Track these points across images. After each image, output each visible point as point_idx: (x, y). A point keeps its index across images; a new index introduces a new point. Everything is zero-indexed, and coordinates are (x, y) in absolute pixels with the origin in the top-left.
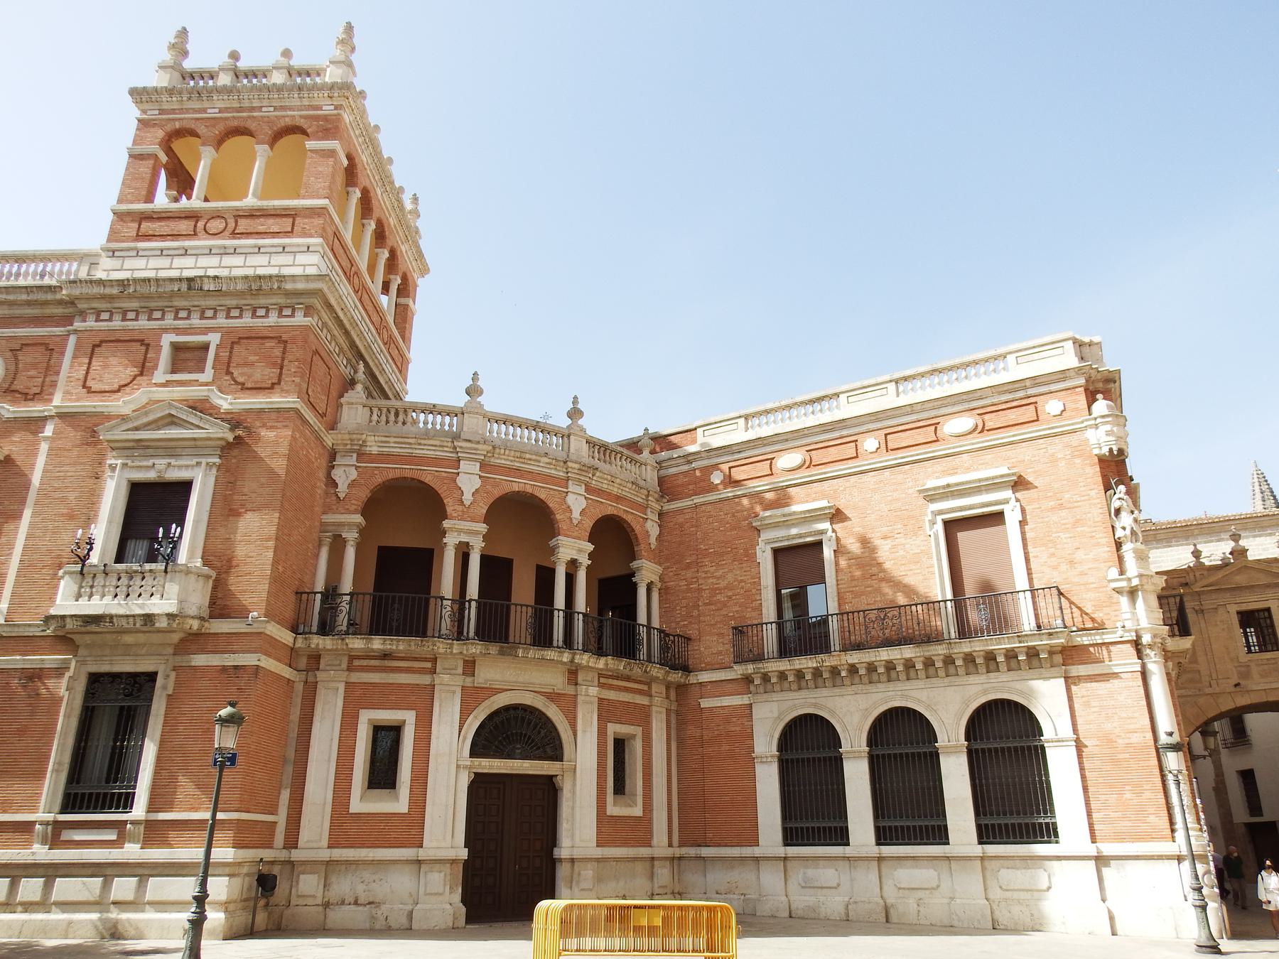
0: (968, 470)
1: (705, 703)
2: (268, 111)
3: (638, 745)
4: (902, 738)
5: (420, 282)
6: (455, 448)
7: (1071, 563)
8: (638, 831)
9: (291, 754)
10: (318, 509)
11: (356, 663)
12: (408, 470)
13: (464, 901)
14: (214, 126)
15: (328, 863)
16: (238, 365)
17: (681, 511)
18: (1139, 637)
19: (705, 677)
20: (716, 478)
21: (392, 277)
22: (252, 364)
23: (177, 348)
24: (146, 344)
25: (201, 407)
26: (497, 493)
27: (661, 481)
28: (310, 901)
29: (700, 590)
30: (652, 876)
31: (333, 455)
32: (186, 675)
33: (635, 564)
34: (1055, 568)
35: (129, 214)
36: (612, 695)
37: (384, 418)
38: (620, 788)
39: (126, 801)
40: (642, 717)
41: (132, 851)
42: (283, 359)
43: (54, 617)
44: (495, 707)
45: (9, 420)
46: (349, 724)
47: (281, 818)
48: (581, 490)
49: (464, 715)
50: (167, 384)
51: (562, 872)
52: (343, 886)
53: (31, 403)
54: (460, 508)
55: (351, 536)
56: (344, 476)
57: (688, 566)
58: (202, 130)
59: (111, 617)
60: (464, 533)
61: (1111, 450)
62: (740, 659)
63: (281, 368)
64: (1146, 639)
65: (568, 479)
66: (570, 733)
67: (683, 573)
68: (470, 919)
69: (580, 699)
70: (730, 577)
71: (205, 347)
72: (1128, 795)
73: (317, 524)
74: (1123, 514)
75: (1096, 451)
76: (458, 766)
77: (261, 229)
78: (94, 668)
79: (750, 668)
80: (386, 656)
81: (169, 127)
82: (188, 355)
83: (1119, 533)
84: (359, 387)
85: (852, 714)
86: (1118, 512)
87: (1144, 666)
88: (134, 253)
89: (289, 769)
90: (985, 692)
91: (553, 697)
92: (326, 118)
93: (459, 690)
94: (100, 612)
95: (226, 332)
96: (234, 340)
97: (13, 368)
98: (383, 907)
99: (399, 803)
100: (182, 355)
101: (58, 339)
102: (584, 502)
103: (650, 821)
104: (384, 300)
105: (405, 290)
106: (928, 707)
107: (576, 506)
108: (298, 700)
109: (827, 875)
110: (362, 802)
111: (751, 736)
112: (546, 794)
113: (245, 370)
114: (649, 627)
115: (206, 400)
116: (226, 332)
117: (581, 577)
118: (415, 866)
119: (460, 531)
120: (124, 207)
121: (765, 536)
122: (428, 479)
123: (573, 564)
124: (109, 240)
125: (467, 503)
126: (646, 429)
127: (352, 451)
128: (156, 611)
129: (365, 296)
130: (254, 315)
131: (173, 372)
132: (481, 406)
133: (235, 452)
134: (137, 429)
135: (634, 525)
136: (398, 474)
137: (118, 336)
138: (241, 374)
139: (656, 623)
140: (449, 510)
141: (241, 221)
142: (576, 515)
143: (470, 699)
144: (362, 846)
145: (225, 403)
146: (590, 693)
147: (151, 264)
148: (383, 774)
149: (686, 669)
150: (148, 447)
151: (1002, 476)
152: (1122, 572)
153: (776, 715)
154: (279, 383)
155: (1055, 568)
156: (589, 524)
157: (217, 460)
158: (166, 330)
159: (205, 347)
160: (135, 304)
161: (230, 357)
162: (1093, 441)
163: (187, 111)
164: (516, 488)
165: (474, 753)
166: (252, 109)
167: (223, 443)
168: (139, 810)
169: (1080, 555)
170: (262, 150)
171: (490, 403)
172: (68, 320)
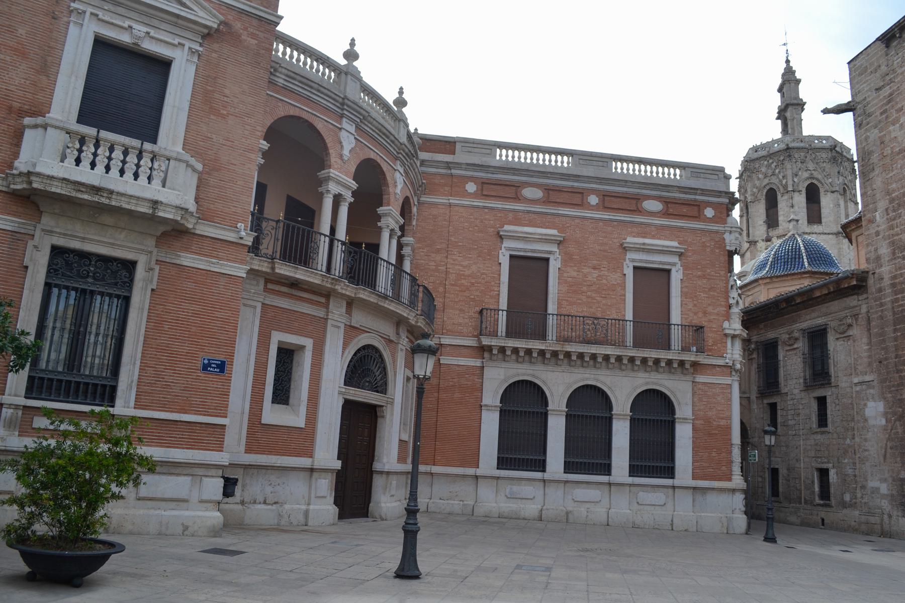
0: (653, 237)
4: (589, 407)
6: (343, 104)
7: (705, 313)
11: (270, 286)
13: (335, 503)
32: (172, 274)
34: (695, 314)
49: (345, 345)
54: (339, 161)
57: (438, 251)
59: (111, 192)
67: (433, 255)
68: (341, 516)
70: (474, 268)
72: (714, 454)
75: (728, 248)
78: (61, 242)
85: (559, 385)
90: (647, 383)
98: (287, 507)
106: (610, 388)
109: (527, 490)
110: (272, 415)
111: (481, 390)
118: (307, 474)
121: (507, 244)
122: (319, 126)
133: (216, 46)
144: (270, 452)
151: (673, 247)
153: (502, 377)
162: (727, 241)
165: (346, 383)
167: (206, 31)
169: (710, 309)
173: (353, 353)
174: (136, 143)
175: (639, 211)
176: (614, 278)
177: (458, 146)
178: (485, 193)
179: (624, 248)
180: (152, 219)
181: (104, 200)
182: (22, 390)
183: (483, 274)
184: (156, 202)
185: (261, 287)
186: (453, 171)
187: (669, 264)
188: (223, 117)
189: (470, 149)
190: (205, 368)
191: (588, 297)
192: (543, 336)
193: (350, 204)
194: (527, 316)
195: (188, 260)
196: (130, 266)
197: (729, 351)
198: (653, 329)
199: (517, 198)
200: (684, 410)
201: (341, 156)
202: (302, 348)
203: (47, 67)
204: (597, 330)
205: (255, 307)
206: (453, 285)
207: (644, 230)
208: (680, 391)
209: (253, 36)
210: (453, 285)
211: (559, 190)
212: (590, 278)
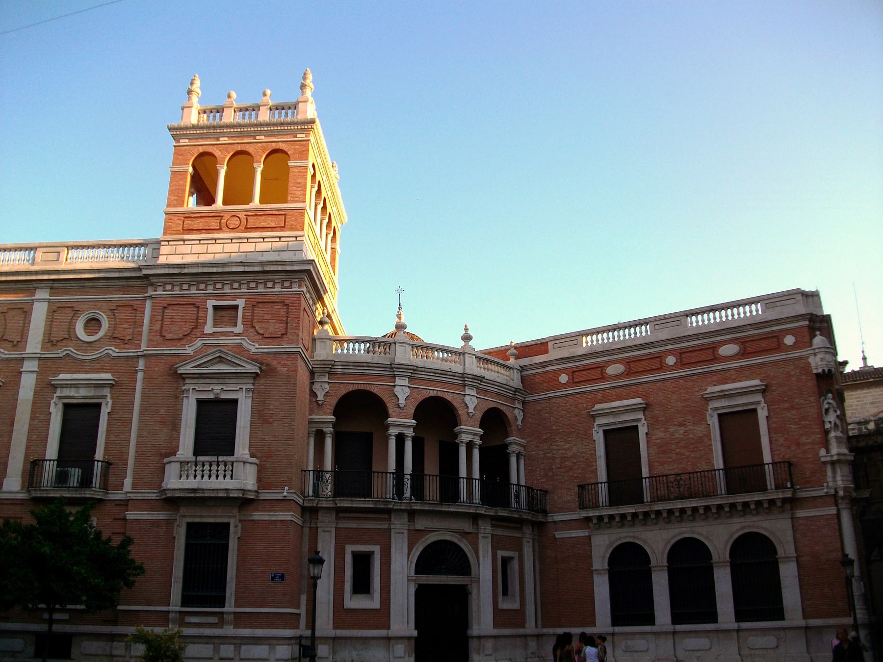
1: (559, 535)
3: (515, 564)
4: (689, 559)
6: (392, 368)
7: (798, 445)
10: (307, 413)
11: (341, 515)
15: (335, 639)
16: (258, 322)
17: (538, 401)
18: (836, 492)
19: (558, 517)
20: (564, 378)
22: (267, 321)
23: (216, 308)
24: (198, 307)
26: (421, 398)
27: (523, 379)
29: (554, 458)
30: (526, 647)
34: (789, 447)
36: (499, 532)
38: (505, 592)
39: (221, 603)
40: (518, 546)
41: (229, 630)
42: (287, 317)
43: (168, 490)
44: (429, 542)
47: (303, 611)
50: (214, 334)
51: (473, 644)
52: (345, 654)
53: (127, 346)
54: (397, 410)
55: (329, 429)
56: (321, 390)
59: (203, 490)
61: (824, 370)
62: (582, 507)
63: (287, 324)
64: (841, 493)
69: (480, 535)
70: (574, 449)
71: (236, 307)
74: (831, 412)
75: (815, 371)
77: (264, 224)
78: (190, 520)
79: (591, 513)
82: (223, 313)
83: (827, 426)
85: (657, 542)
86: (827, 411)
87: (838, 510)
88: (182, 243)
91: (464, 534)
93: (406, 532)
96: (255, 303)
97: (113, 322)
99: (372, 602)
101: (139, 302)
107: (471, 403)
113: (263, 325)
115: (240, 345)
116: (248, 297)
117: (476, 453)
122: (375, 390)
123: (470, 445)
128: (230, 487)
130: (266, 287)
133: (262, 381)
135: (507, 413)
136: (356, 387)
137: (178, 301)
138: (262, 328)
139: (523, 483)
140: (391, 411)
142: (471, 410)
143: (414, 536)
145: (253, 347)
148: (362, 586)
150: (207, 378)
151: (756, 386)
152: (828, 451)
153: (607, 542)
154: (286, 334)
155: (789, 447)
156: (479, 415)
159: (236, 307)
161: (252, 316)
162: (813, 364)
164: (432, 394)
165: (416, 572)
168: (230, 607)
169: (803, 439)
172: (144, 289)
173: (421, 549)
174: (214, 458)
175: (716, 359)
176: (699, 430)
177: (550, 345)
178: (576, 380)
179: (705, 399)
181: (201, 495)
183: (583, 452)
184: (227, 490)
185: (334, 517)
186: (547, 369)
187: (752, 403)
188: (271, 423)
190: (273, 579)
191: (677, 454)
192: (640, 500)
193: (414, 438)
194: (625, 482)
195: (258, 516)
197: (829, 479)
198: (743, 473)
199: (603, 378)
200: (786, 547)
201: (398, 406)
202: (373, 552)
203: (175, 426)
204: (688, 484)
205: (330, 531)
206: (558, 468)
207: (724, 377)
208: (777, 528)
209: (284, 365)
210: (558, 468)
211: (638, 360)
212: (677, 436)
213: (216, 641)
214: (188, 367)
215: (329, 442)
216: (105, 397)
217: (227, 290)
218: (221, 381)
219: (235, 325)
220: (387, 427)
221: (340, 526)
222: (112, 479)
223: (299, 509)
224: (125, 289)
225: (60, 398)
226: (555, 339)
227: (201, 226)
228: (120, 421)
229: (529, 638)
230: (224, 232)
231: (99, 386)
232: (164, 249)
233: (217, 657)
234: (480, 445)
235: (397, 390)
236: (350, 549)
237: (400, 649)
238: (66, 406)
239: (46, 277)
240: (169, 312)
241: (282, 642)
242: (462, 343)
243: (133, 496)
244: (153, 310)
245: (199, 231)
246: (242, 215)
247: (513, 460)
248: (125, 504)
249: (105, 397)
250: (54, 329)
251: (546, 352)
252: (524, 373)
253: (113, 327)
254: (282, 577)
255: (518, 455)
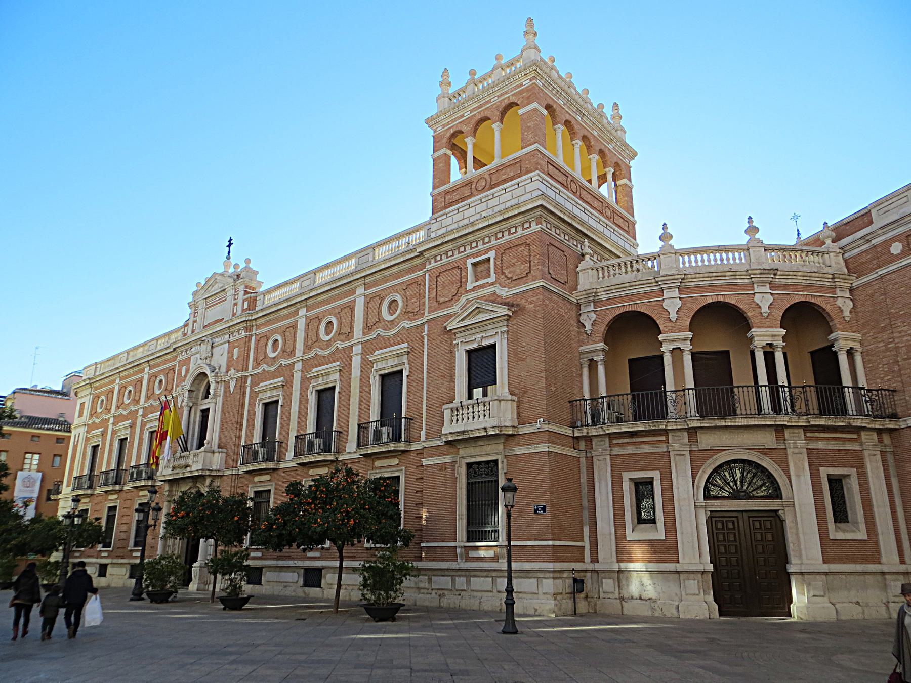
2: (495, 100)
5: (632, 163)
6: (657, 282)
8: (867, 550)
9: (585, 503)
11: (615, 442)
12: (627, 306)
14: (469, 123)
16: (507, 267)
21: (607, 169)
22: (514, 265)
23: (474, 265)
24: (461, 268)
25: (494, 299)
26: (696, 308)
28: (611, 596)
29: (897, 348)
31: (579, 305)
33: (832, 336)
35: (439, 194)
37: (606, 274)
38: (841, 515)
45: (409, 329)
46: (617, 482)
47: (587, 543)
48: (767, 289)
54: (670, 324)
55: (599, 357)
57: (883, 329)
58: (464, 128)
60: (676, 341)
65: (753, 283)
66: (785, 477)
67: (879, 336)
69: (789, 451)
71: (489, 260)
73: (577, 354)
76: (696, 507)
80: (633, 434)
81: (448, 135)
84: (587, 258)
89: (586, 514)
92: (528, 89)
93: (688, 454)
94: (462, 429)
95: (497, 248)
96: (502, 251)
100: (480, 268)
102: (771, 299)
103: (877, 543)
104: (604, 190)
105: (621, 171)
107: (763, 302)
108: (584, 470)
112: (774, 524)
113: (511, 269)
114: (856, 388)
115: (494, 293)
118: (677, 576)
119: (672, 341)
120: (436, 191)
124: (433, 213)
125: (674, 319)
126: (825, 223)
127: (589, 302)
129: (584, 193)
131: (477, 281)
132: (672, 247)
133: (515, 322)
134: (463, 319)
138: (509, 272)
139: (862, 382)
140: (661, 327)
141: (494, 177)
146: (797, 443)
147: (459, 218)
149: (894, 416)
150: (471, 329)
157: (505, 329)
158: (467, 257)
159: (489, 260)
160: (450, 246)
163: (455, 120)
166: (487, 102)
170: (496, 126)
171: (677, 243)
172: (423, 265)
177: (874, 213)
180: (487, 437)
182: (465, 539)
184: (485, 428)
186: (873, 242)
188: (524, 360)
189: (886, 209)
190: (536, 511)
195: (519, 451)
196: (496, 462)
206: (905, 359)
210: (905, 359)
213: (494, 574)
214: (454, 323)
215: (601, 369)
216: (403, 364)
217: (481, 247)
218: (482, 329)
219: (489, 276)
220: (661, 343)
221: (614, 453)
222: (414, 433)
223: (571, 439)
224: (411, 270)
225: (377, 371)
226: (878, 203)
227: (458, 197)
228: (416, 382)
229: (887, 577)
230: (475, 196)
231: (399, 355)
232: (434, 227)
233: (495, 591)
234: (783, 347)
235: (665, 304)
236: (626, 476)
237: (692, 585)
238: (383, 377)
239: (358, 276)
240: (440, 279)
241: (548, 575)
242: (748, 238)
243: (426, 444)
244: (429, 281)
245: (457, 202)
246: (487, 176)
247: (843, 359)
248: (420, 453)
249: (403, 364)
250: (370, 317)
251: (871, 222)
252: (847, 255)
253: (406, 304)
254: (544, 509)
255: (850, 353)
